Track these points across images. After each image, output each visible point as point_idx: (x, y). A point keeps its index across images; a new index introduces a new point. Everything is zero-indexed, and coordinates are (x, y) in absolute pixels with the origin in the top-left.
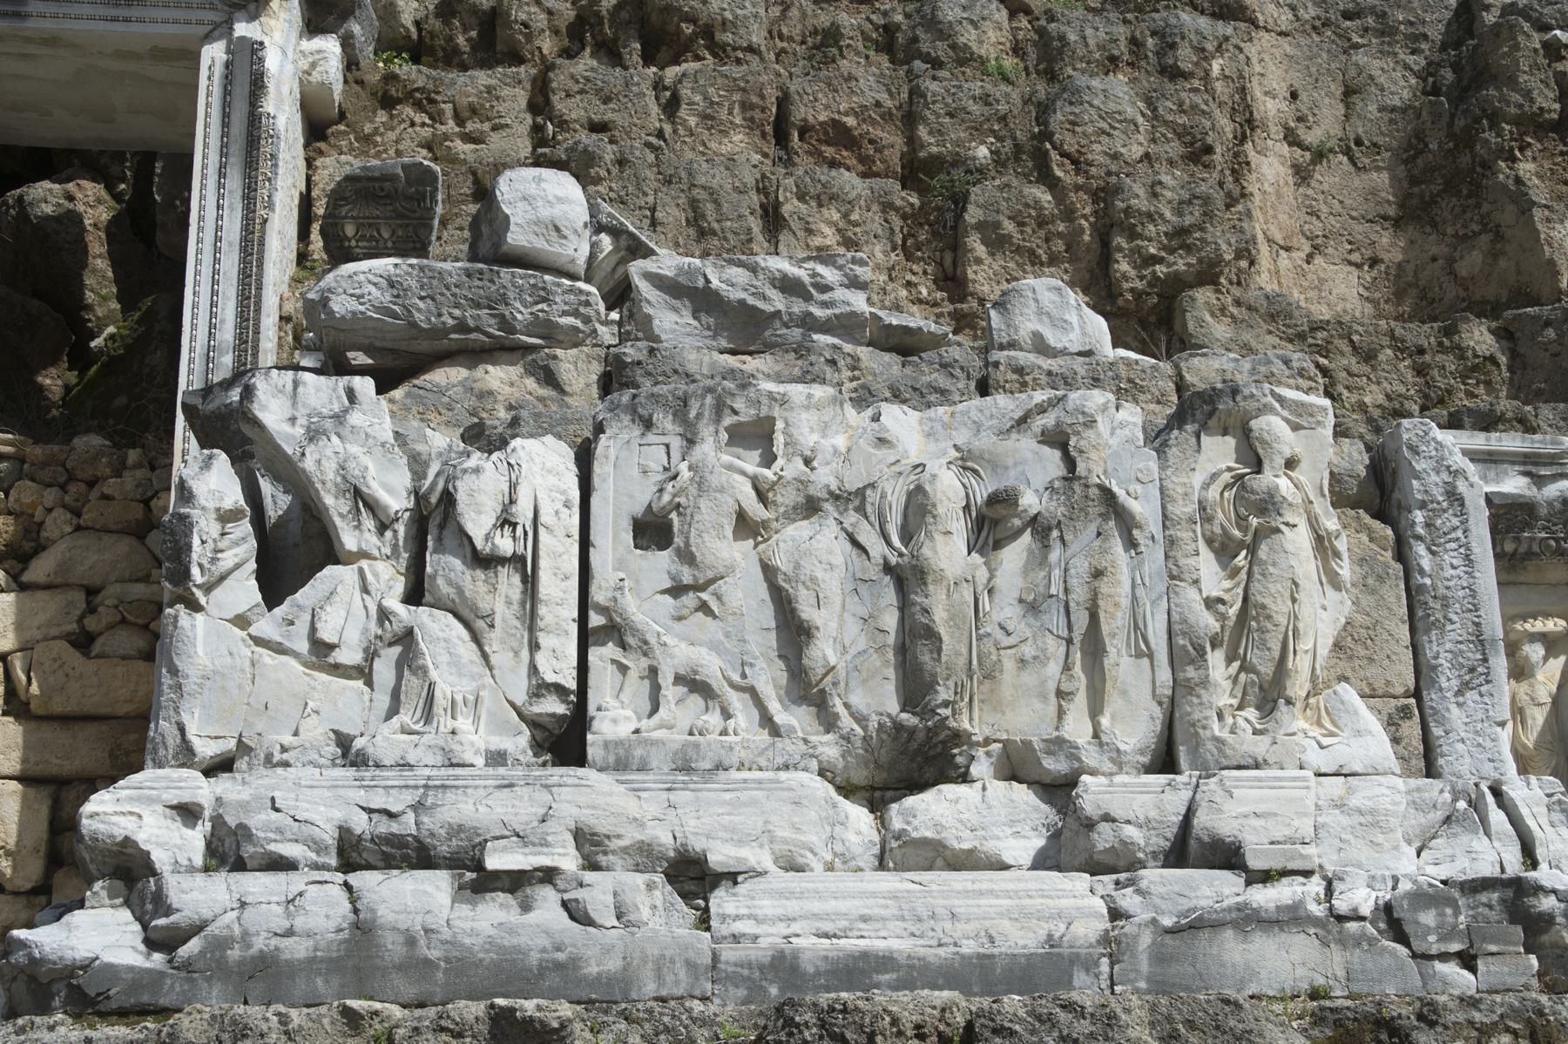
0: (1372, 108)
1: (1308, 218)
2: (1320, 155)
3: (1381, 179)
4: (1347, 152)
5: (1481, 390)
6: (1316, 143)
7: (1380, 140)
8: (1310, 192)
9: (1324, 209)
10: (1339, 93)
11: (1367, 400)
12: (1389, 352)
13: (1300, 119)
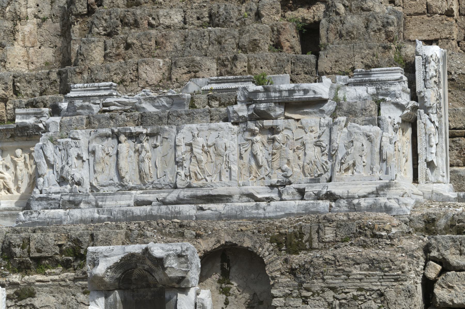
0: (57, 6)
1: (40, 37)
2: (44, 20)
3: (58, 25)
4: (51, 18)
5: (54, 88)
6: (43, 17)
7: (58, 15)
8: (41, 30)
9: (44, 34)
10: (49, 3)
11: (28, 93)
12: (34, 80)
13: (39, 11)
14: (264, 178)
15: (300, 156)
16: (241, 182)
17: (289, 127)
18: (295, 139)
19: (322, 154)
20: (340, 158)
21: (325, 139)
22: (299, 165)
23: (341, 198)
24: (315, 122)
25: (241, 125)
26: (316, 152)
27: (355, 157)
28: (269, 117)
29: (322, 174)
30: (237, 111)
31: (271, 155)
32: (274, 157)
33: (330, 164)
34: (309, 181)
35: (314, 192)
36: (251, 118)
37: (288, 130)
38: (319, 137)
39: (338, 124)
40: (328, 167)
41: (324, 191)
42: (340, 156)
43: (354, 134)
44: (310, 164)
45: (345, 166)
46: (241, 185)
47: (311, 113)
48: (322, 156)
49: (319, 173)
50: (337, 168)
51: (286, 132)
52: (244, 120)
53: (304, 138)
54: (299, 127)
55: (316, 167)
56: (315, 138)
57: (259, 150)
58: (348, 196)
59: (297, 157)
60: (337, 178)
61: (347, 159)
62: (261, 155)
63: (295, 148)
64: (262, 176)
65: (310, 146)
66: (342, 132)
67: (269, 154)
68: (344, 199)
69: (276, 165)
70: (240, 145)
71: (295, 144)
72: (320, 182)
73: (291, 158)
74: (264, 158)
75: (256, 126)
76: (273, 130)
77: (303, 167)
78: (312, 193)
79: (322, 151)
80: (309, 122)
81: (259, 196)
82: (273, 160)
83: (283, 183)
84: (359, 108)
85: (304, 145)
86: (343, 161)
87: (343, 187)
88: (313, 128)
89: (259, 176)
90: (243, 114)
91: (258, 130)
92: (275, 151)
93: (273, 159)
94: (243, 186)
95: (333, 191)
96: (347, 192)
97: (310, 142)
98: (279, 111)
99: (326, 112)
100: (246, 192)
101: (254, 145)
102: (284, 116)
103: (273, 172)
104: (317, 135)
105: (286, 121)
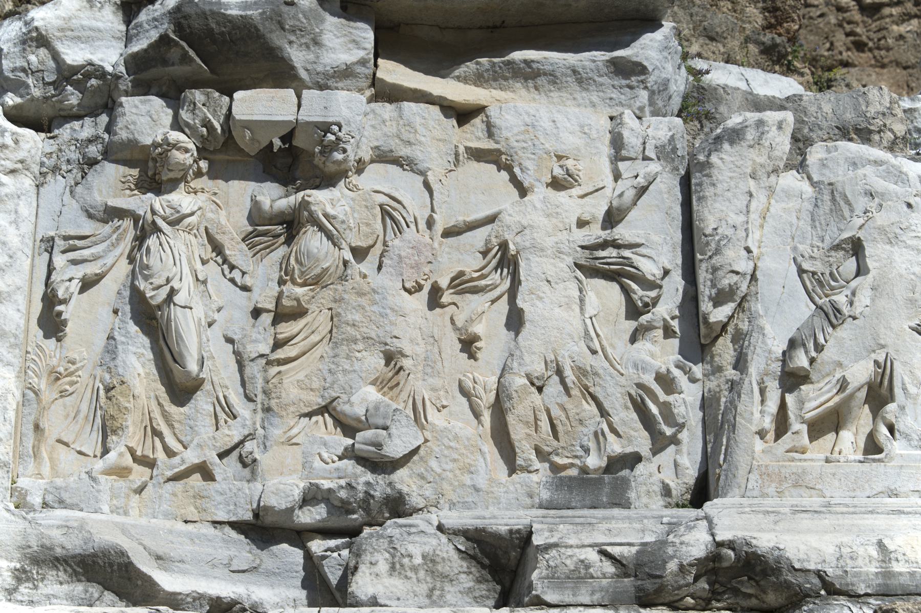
14: (205, 472)
15: (478, 329)
16: (34, 487)
17: (404, 151)
18: (439, 228)
19: (632, 325)
20: (779, 347)
21: (656, 238)
22: (464, 392)
23: (832, 590)
24: (584, 131)
25: (65, 132)
26: (590, 311)
27: (887, 338)
28: (281, 74)
29: (634, 459)
30: (53, 34)
31: (267, 319)
32: (286, 329)
33: (687, 400)
34: (545, 495)
35: (615, 551)
36: (151, 72)
37: (393, 169)
38: (612, 218)
39: (751, 135)
40: (679, 411)
41: (696, 543)
42: (772, 338)
43: (861, 203)
44: (553, 388)
45: (816, 398)
46: (36, 499)
47: (553, 78)
48: (633, 339)
49: (615, 447)
50: (756, 413)
51: (378, 180)
52: (100, 94)
53: (506, 218)
54: (478, 155)
55: (590, 408)
56: (582, 224)
57: (188, 279)
58: (888, 575)
59: (451, 344)
60: (766, 474)
61: (830, 353)
62: (199, 311)
63: (444, 283)
64: (192, 457)
65: (551, 272)
66: (771, 190)
67: (256, 313)
68: (854, 596)
69: (297, 384)
70: (49, 244)
71: (443, 259)
72: (626, 505)
73: (411, 345)
74: (215, 335)
75: (177, 125)
76: (297, 159)
77: (499, 410)
78: (592, 555)
79: (634, 311)
80: (547, 125)
81: (167, 582)
82: (281, 354)
83: (344, 508)
84: (825, 124)
85: (508, 261)
86: (801, 360)
87: (827, 521)
88: (570, 163)
89: (170, 453)
90: (96, 58)
91: (191, 146)
92: (300, 291)
93: (278, 345)
94: (45, 505)
95: (765, 541)
96: (874, 552)
97: (549, 242)
98: (346, 42)
99: (651, 80)
100: (74, 544)
101: (152, 242)
102: (374, 81)
103: (276, 432)
104: (598, 208)
105: (386, 110)
